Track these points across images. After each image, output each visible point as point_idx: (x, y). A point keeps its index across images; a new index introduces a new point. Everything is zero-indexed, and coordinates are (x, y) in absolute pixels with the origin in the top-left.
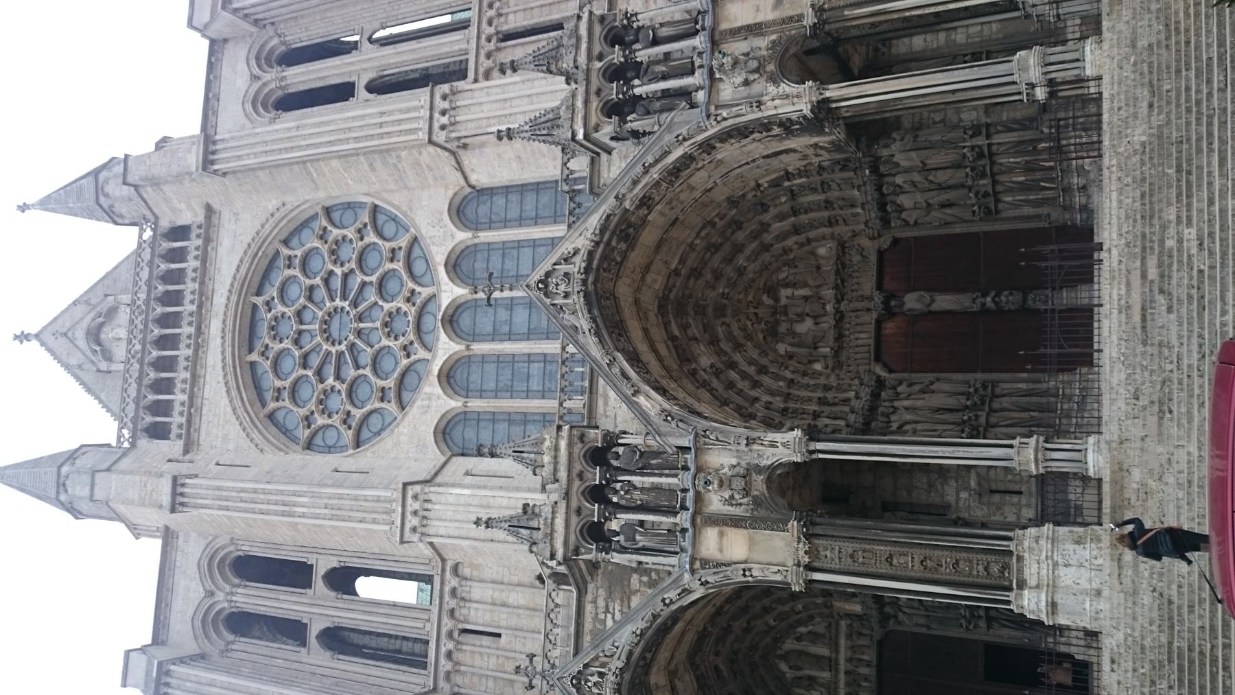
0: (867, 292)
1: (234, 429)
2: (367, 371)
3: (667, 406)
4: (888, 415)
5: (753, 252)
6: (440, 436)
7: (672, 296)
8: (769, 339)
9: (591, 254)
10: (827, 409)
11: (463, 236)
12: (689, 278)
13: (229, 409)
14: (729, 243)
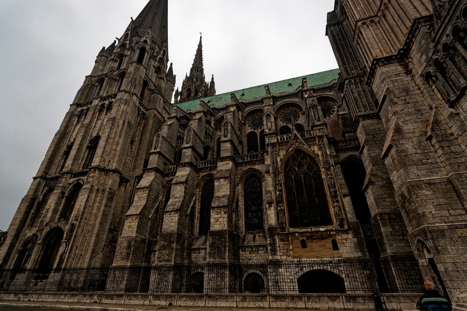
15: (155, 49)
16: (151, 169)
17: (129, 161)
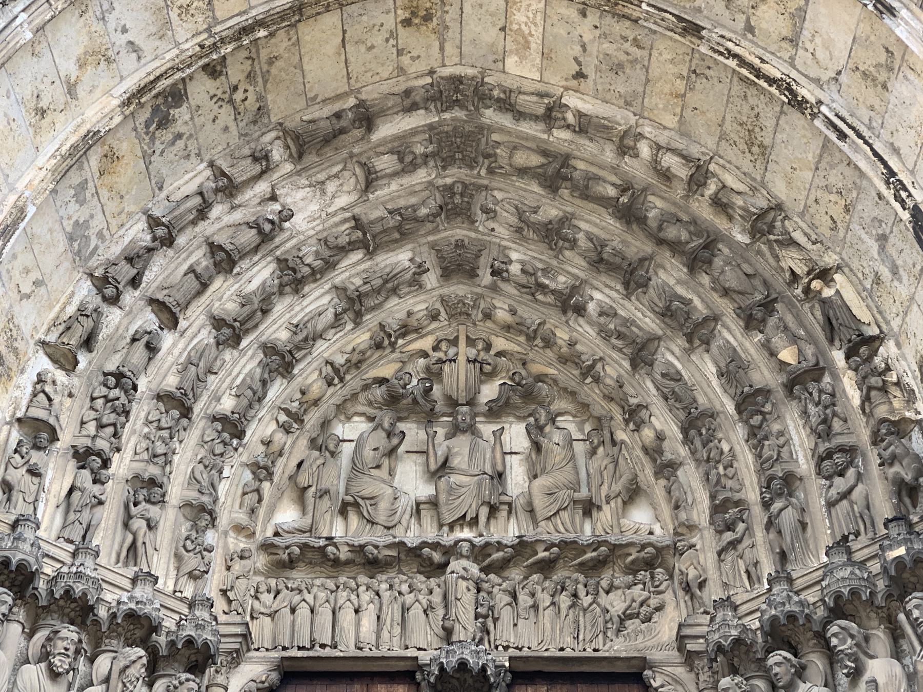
0: (505, 632)
4: (45, 656)
5: (628, 322)
7: (490, 116)
8: (379, 392)
10: (115, 492)
12: (545, 153)
14: (648, 248)
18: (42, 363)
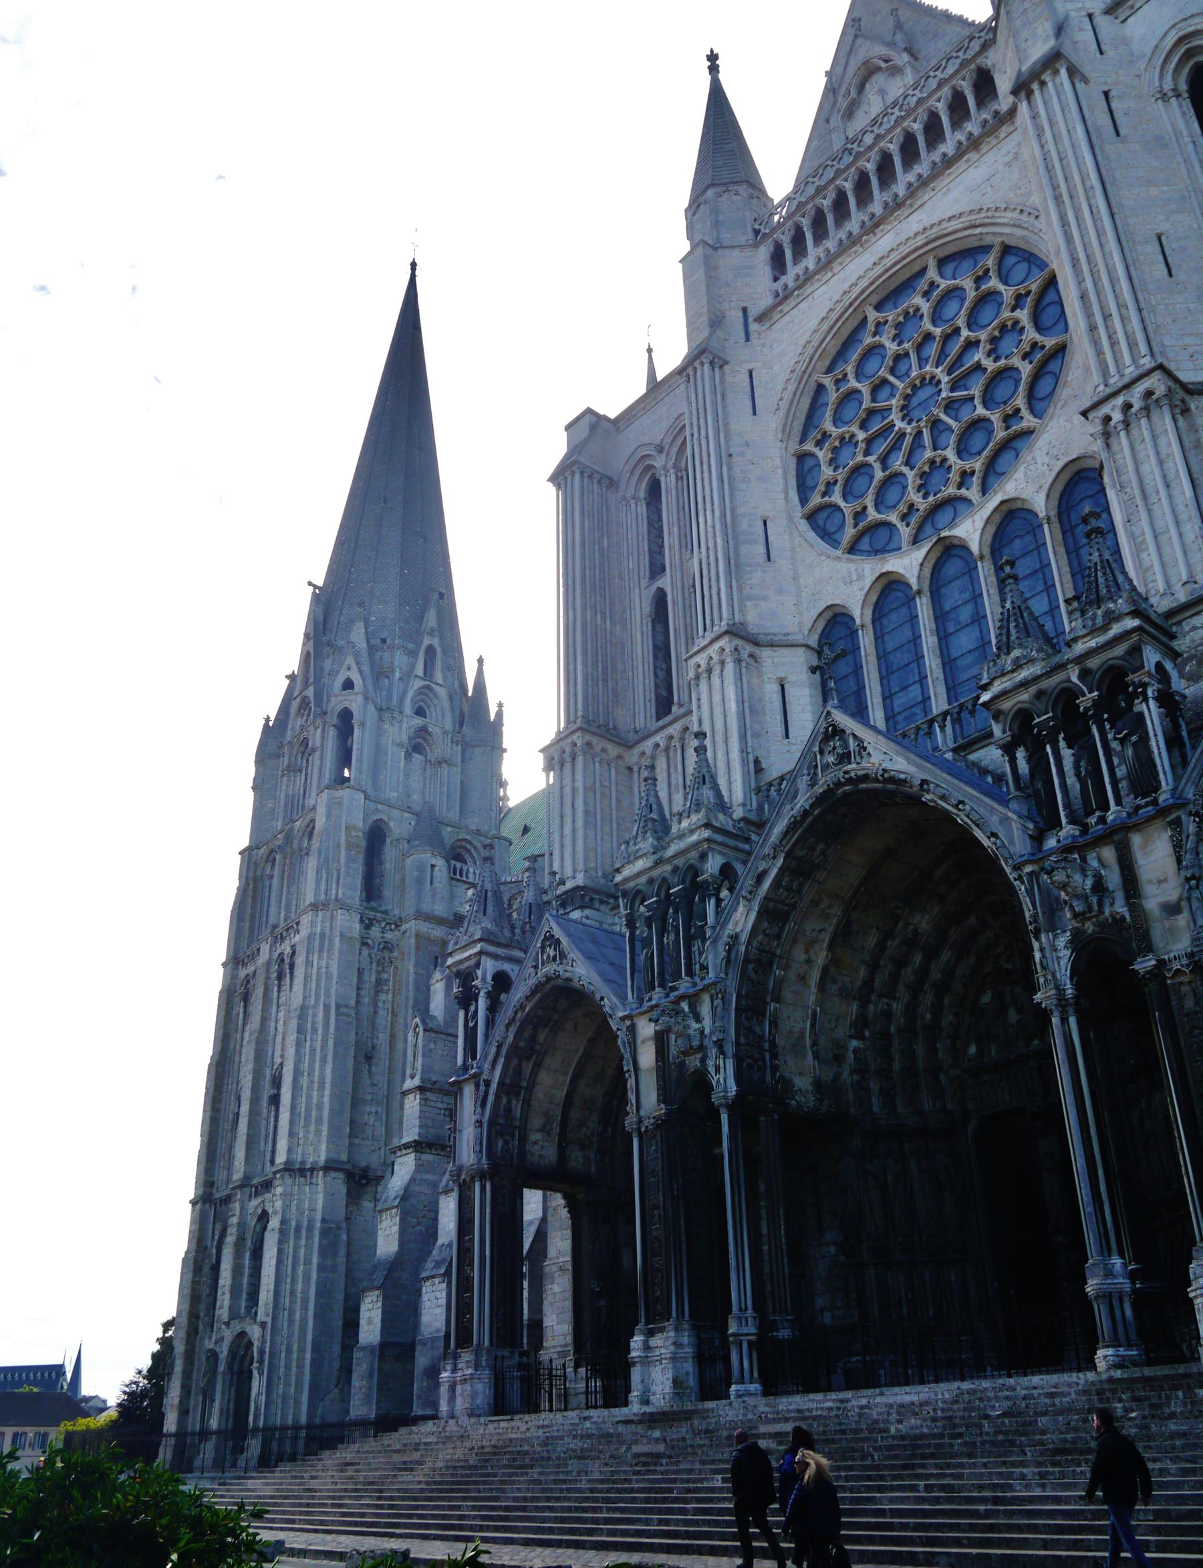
1: (789, 361)
2: (879, 474)
3: (744, 938)
6: (829, 615)
9: (865, 778)
11: (1040, 504)
13: (806, 338)
15: (393, 671)
16: (406, 1146)
17: (372, 1119)
18: (854, 1043)
